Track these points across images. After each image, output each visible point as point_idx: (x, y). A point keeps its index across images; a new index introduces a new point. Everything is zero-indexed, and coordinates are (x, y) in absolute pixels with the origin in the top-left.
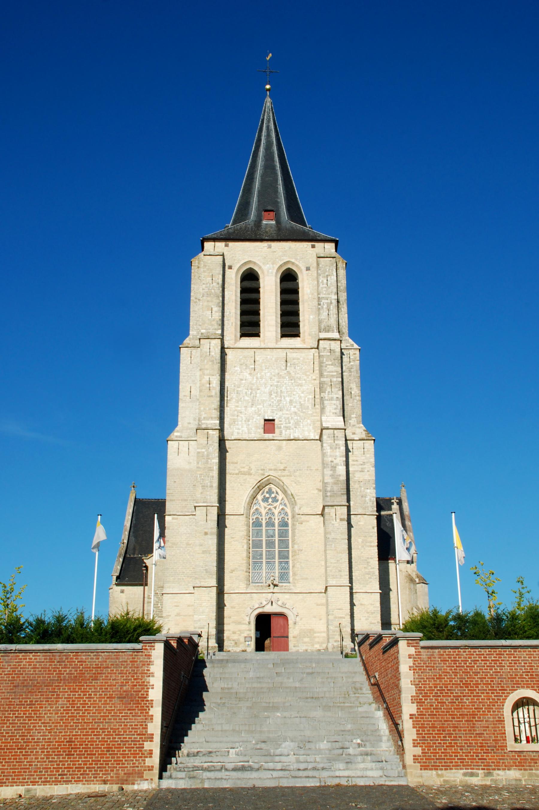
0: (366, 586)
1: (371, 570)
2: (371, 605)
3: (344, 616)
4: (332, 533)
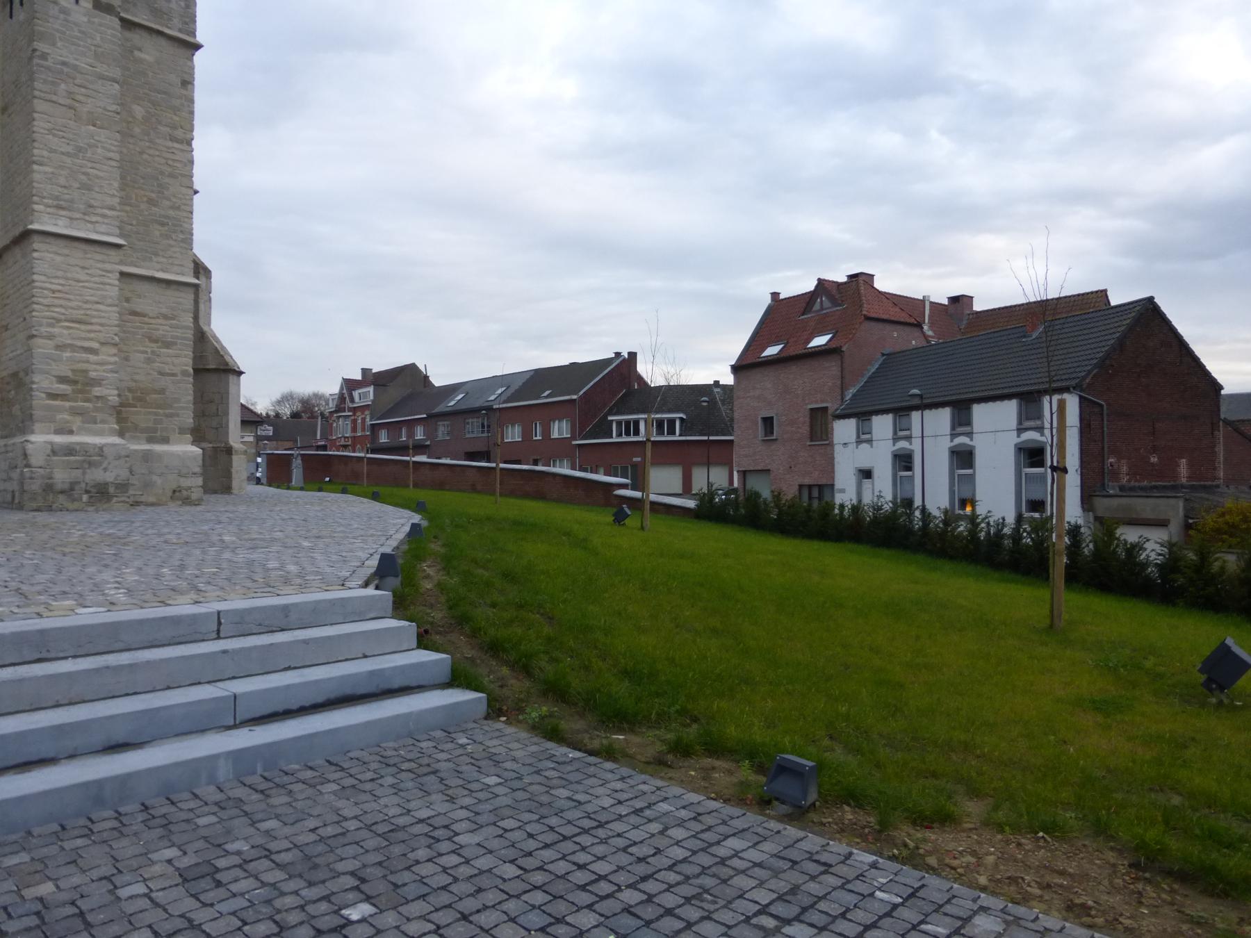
0: (151, 259)
1: (171, 213)
2: (166, 317)
3: (95, 345)
4: (59, 44)
